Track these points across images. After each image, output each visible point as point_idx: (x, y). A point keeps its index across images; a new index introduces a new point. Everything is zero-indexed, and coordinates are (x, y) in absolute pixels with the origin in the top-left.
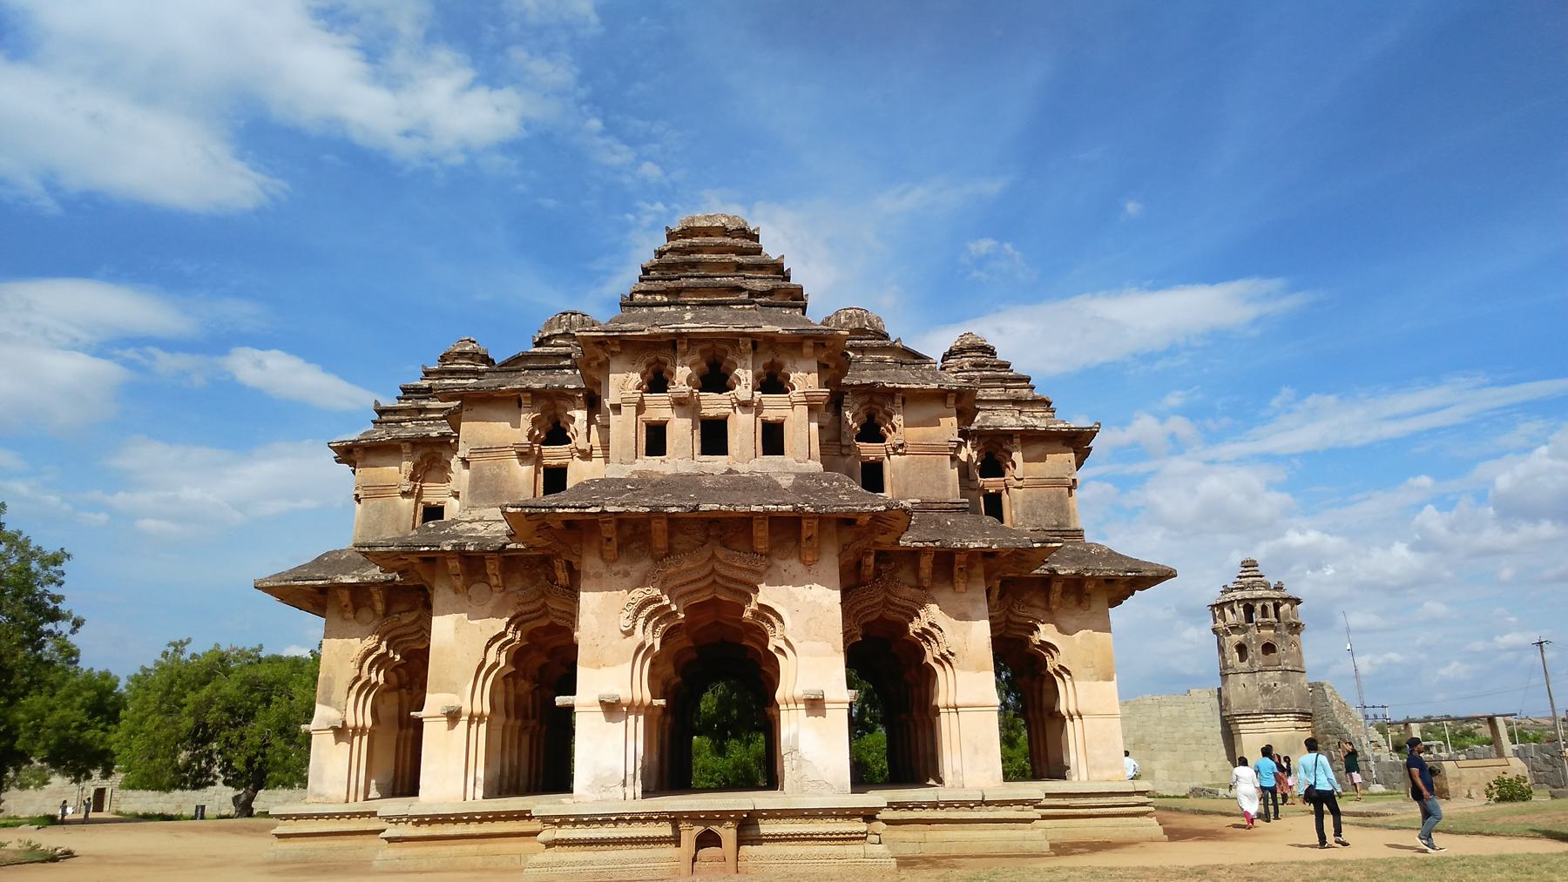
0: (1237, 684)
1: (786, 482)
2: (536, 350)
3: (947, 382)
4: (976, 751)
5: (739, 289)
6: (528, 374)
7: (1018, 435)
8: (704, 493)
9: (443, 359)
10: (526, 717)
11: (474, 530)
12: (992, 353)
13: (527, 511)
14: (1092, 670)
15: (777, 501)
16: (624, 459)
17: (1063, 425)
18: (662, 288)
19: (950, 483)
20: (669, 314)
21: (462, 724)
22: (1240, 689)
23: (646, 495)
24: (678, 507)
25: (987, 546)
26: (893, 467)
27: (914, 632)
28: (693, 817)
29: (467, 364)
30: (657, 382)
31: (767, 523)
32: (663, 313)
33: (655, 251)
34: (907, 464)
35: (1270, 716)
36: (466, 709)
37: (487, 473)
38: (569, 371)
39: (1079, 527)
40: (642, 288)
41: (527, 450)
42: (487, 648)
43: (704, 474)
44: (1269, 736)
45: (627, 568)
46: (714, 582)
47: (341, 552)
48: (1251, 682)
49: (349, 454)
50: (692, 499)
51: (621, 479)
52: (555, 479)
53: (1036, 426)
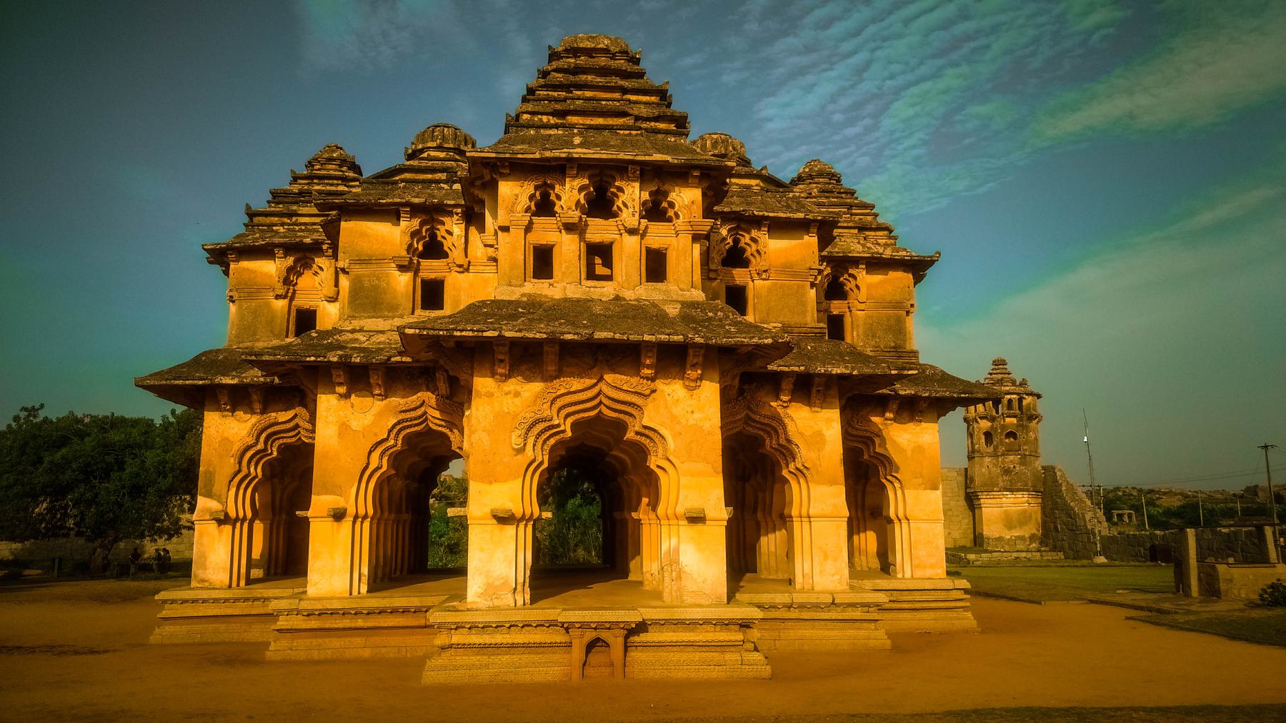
0: (981, 465)
1: (673, 311)
2: (408, 163)
3: (811, 212)
4: (826, 557)
5: (624, 114)
6: (404, 187)
7: (864, 261)
8: (597, 322)
9: (310, 164)
10: (399, 511)
11: (356, 340)
12: (838, 181)
13: (425, 333)
14: (920, 480)
15: (668, 331)
16: (514, 282)
17: (904, 253)
18: (549, 110)
19: (809, 308)
20: (558, 137)
21: (347, 523)
23: (540, 320)
24: (574, 334)
25: (849, 372)
26: (757, 288)
27: (771, 447)
28: (584, 626)
29: (335, 170)
30: (544, 206)
31: (655, 351)
32: (550, 135)
33: (538, 70)
34: (770, 290)
35: (1008, 493)
36: (351, 510)
37: (366, 284)
38: (446, 186)
39: (915, 348)
40: (530, 109)
41: (406, 263)
42: (370, 452)
43: (592, 300)
44: (1006, 510)
45: (518, 388)
46: (601, 402)
47: (218, 351)
48: (994, 465)
49: (221, 256)
50: (585, 327)
51: (512, 302)
52: (432, 294)
53: (882, 254)
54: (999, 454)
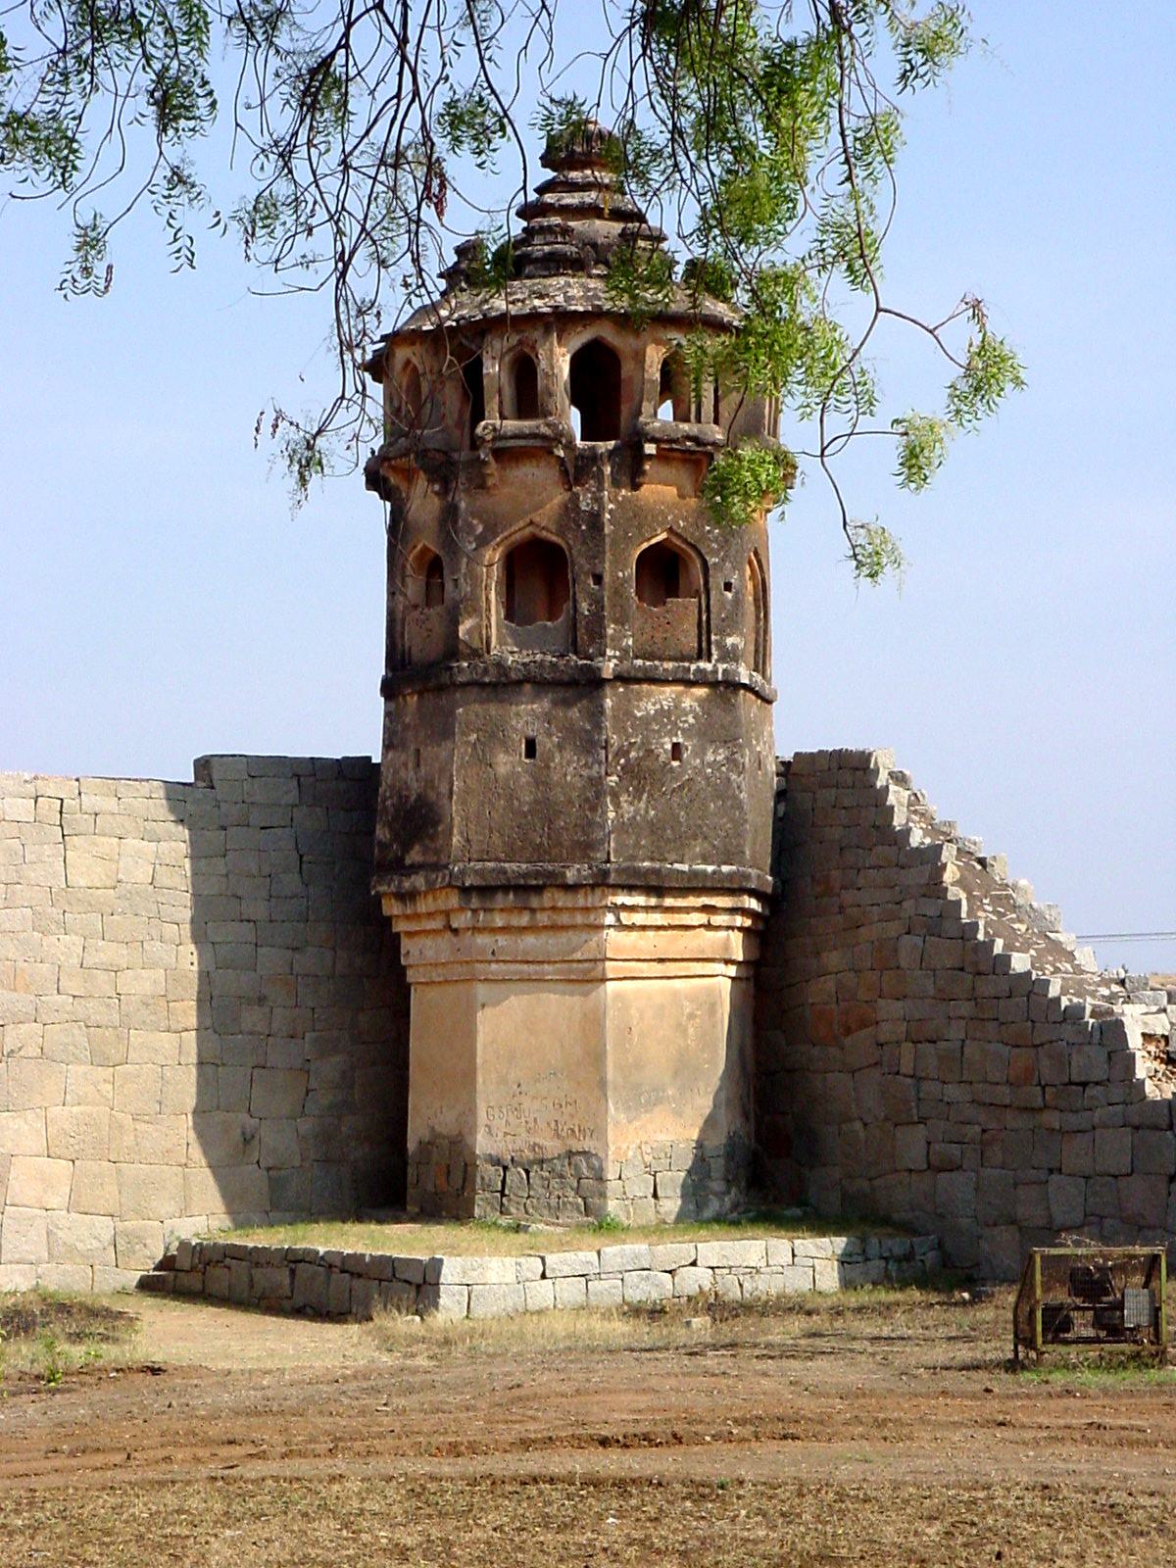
0: (495, 736)
22: (507, 763)
35: (640, 900)
48: (570, 731)
54: (609, 668)
